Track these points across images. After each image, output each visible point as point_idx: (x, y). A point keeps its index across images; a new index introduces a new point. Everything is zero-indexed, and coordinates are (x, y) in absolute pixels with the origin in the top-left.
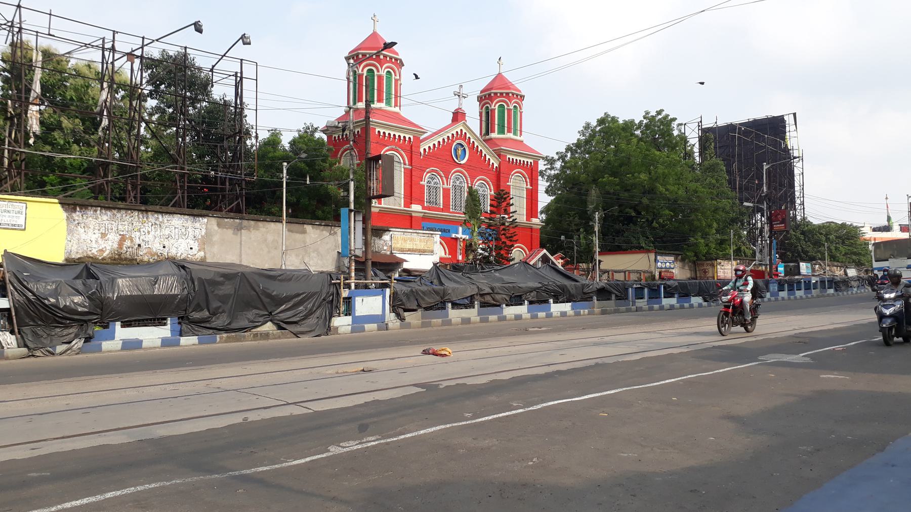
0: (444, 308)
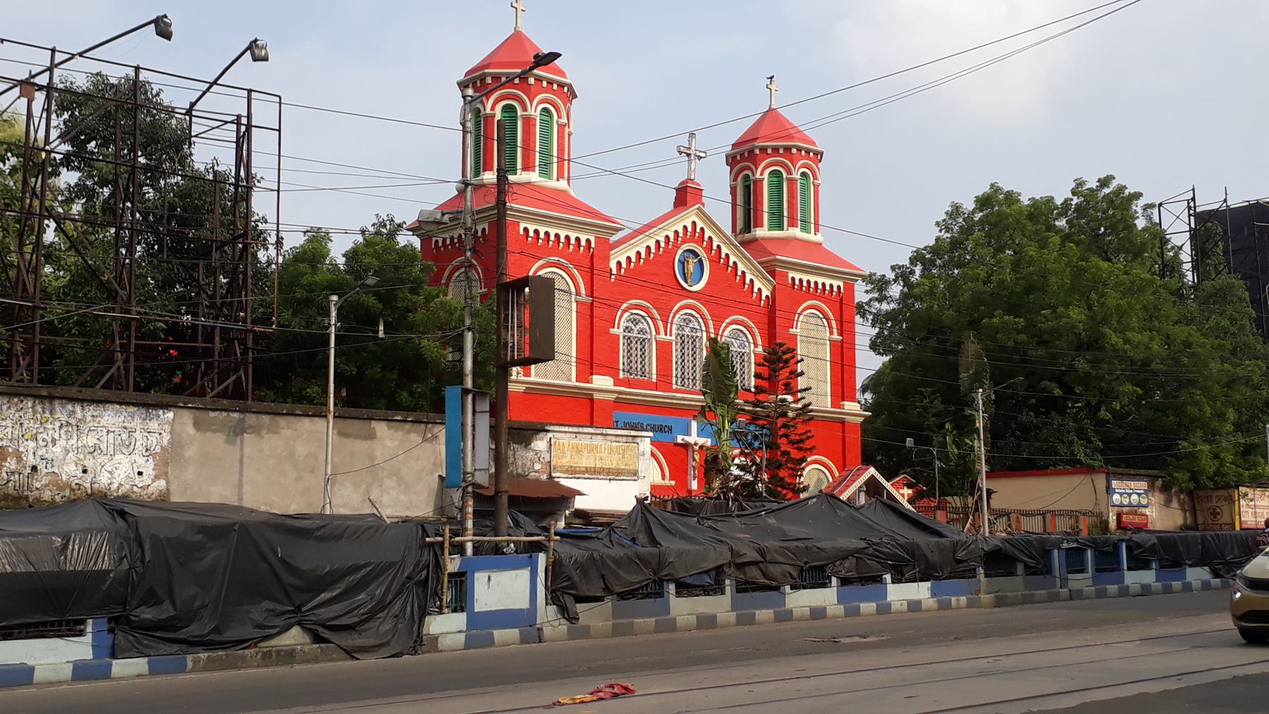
0: (660, 594)
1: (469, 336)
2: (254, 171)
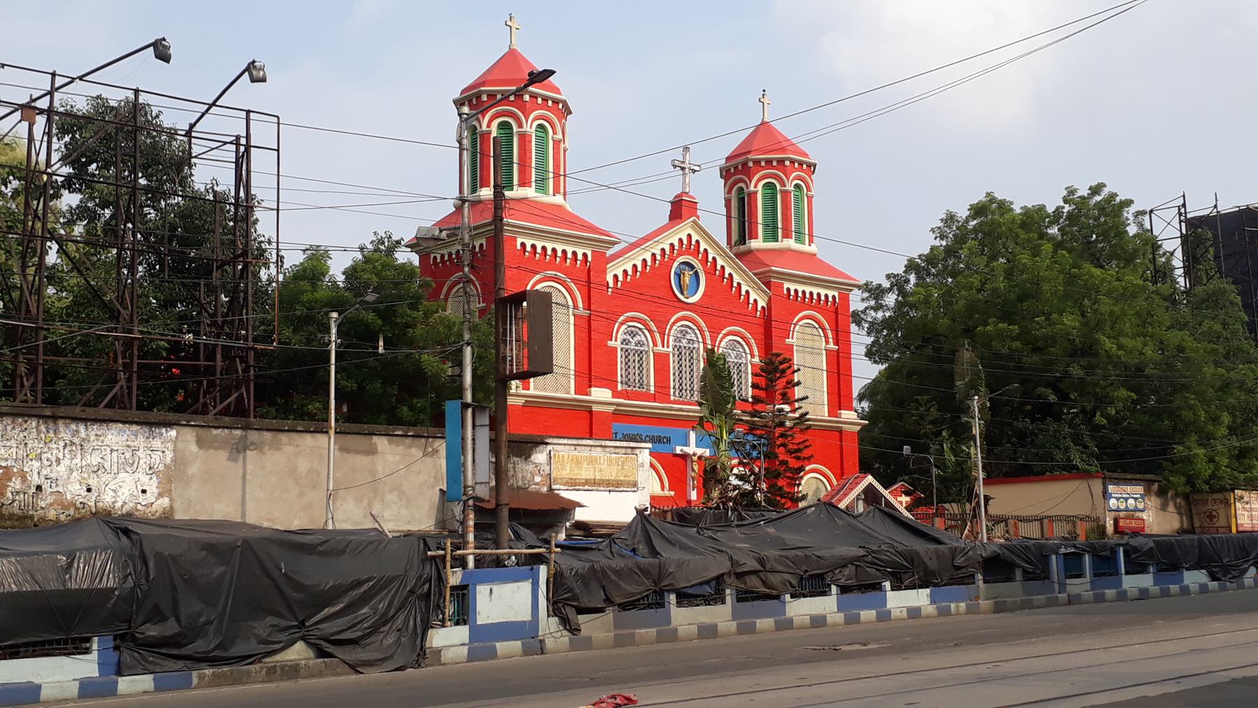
0: (661, 604)
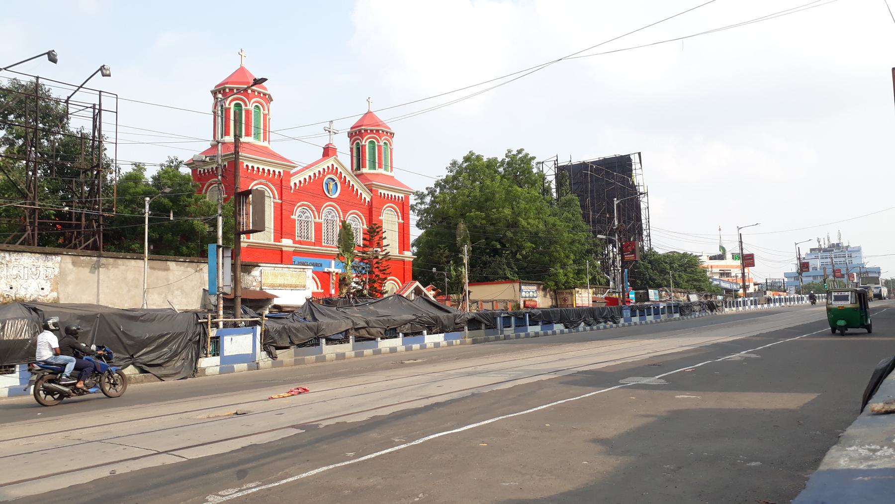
0: (318, 344)
1: (220, 219)
2: (103, 133)
